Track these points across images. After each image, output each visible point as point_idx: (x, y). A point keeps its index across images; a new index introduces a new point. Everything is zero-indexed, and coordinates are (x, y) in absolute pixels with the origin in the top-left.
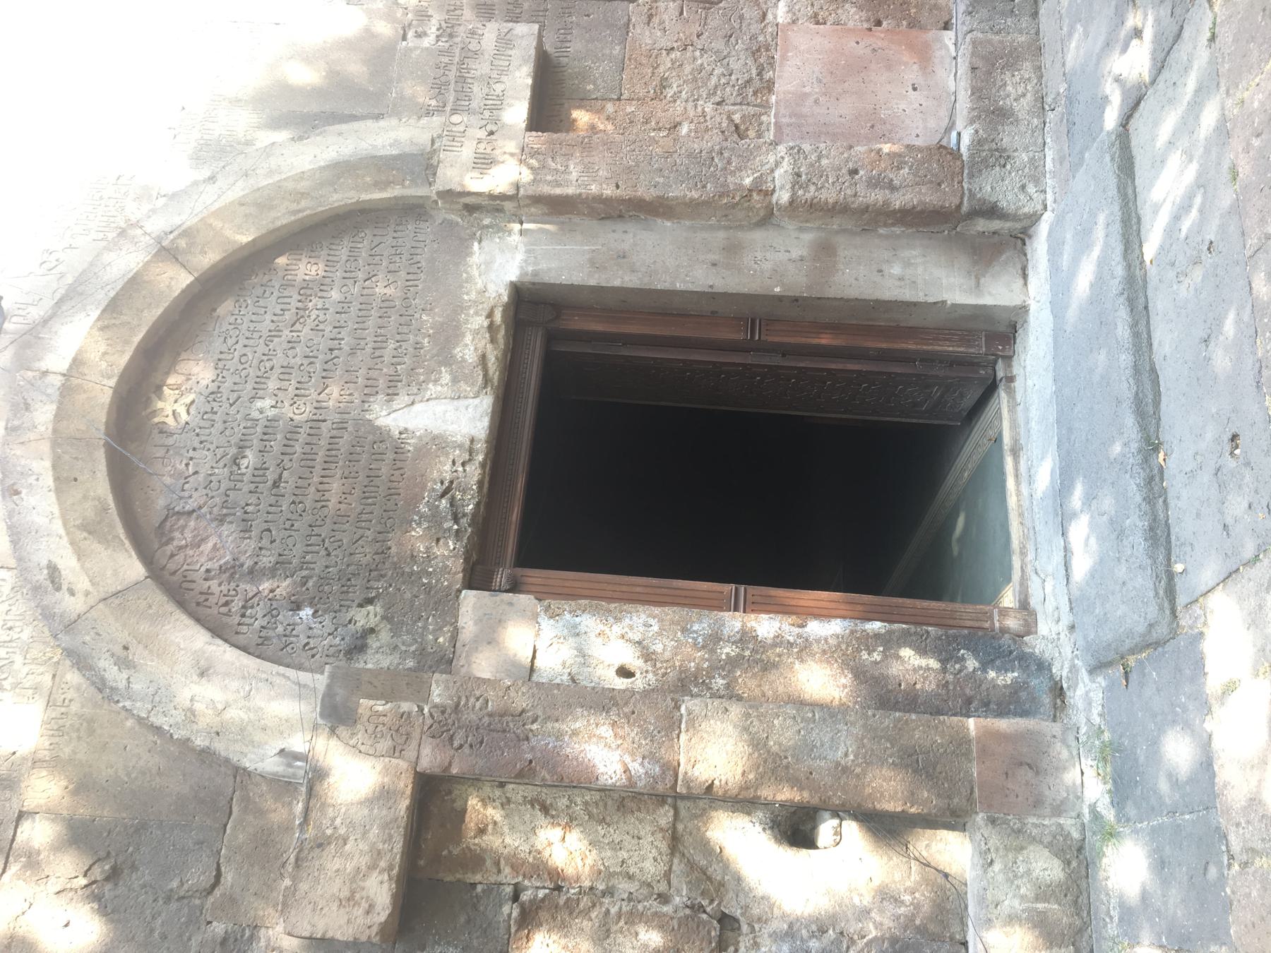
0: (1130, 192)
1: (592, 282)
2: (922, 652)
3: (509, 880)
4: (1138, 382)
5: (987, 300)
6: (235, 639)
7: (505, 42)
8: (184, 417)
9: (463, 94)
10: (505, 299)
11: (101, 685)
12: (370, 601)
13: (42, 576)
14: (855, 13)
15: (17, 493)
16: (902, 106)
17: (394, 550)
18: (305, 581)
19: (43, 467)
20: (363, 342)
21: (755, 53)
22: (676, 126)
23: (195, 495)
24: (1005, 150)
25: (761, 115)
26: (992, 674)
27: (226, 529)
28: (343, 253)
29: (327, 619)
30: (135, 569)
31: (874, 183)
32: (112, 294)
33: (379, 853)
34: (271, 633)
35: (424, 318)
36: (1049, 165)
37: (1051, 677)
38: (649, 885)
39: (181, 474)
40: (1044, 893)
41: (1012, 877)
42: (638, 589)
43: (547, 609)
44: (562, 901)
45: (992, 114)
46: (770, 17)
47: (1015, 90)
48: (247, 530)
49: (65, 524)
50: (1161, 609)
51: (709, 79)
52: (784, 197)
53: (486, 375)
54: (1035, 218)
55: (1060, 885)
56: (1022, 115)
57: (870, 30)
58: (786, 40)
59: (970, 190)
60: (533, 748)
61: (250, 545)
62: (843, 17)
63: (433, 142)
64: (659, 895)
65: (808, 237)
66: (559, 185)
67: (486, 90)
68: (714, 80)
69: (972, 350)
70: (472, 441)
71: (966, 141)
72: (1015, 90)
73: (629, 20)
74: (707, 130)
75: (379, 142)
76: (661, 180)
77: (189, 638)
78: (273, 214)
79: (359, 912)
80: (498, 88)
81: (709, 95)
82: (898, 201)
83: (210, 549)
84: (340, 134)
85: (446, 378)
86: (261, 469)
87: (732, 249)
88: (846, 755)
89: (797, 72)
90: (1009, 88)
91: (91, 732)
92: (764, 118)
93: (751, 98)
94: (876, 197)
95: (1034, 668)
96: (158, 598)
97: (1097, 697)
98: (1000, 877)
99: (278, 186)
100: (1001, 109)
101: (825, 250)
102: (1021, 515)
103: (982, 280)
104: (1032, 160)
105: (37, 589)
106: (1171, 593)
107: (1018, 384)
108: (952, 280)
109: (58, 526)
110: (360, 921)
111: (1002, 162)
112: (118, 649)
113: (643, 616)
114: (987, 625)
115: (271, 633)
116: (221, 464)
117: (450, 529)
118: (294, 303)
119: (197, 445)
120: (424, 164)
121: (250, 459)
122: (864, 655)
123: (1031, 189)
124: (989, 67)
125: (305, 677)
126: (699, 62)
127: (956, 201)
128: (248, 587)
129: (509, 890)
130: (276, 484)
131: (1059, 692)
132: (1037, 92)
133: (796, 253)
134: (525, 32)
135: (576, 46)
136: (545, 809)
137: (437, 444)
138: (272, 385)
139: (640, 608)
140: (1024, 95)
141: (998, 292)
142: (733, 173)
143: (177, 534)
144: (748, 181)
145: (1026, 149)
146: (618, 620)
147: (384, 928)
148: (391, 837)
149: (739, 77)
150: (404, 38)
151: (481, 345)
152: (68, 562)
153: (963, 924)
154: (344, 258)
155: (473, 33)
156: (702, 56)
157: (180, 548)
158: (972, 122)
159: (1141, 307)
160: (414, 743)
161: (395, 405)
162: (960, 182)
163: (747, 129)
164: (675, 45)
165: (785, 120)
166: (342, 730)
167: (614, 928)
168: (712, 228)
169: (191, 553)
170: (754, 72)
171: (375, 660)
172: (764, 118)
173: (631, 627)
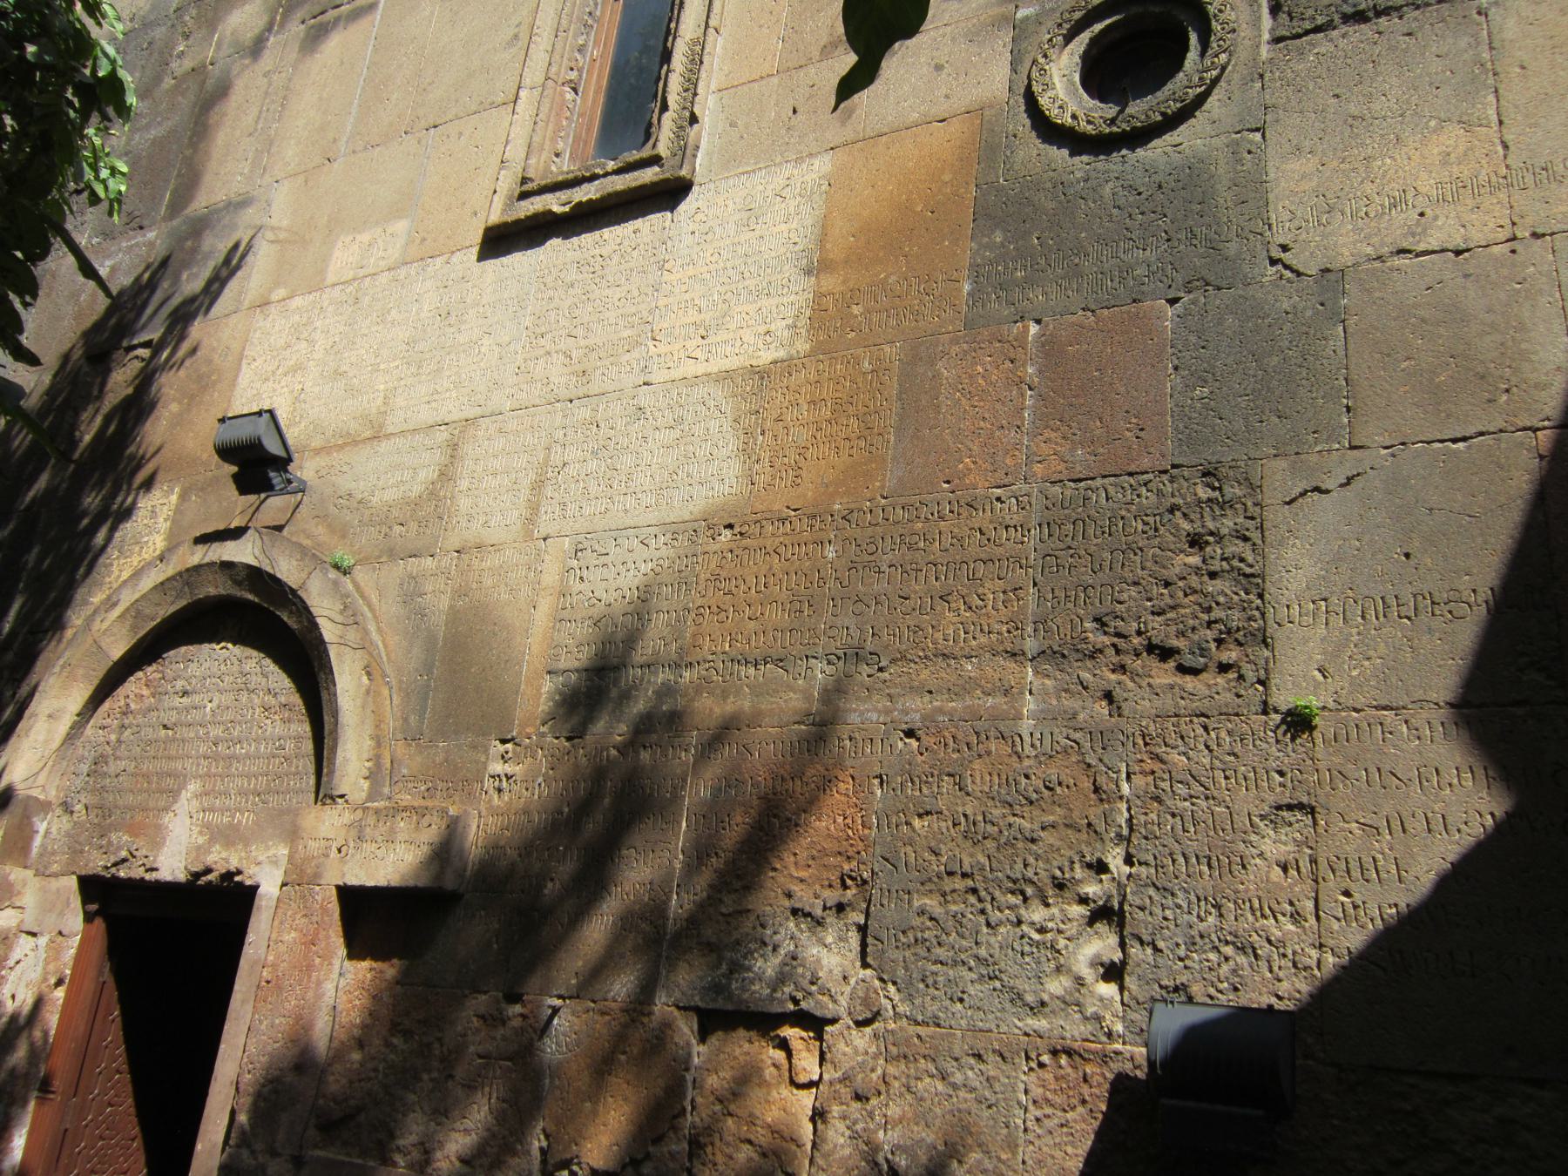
63: (342, 796)
85: (201, 840)
151: (218, 867)
156: (431, 1080)
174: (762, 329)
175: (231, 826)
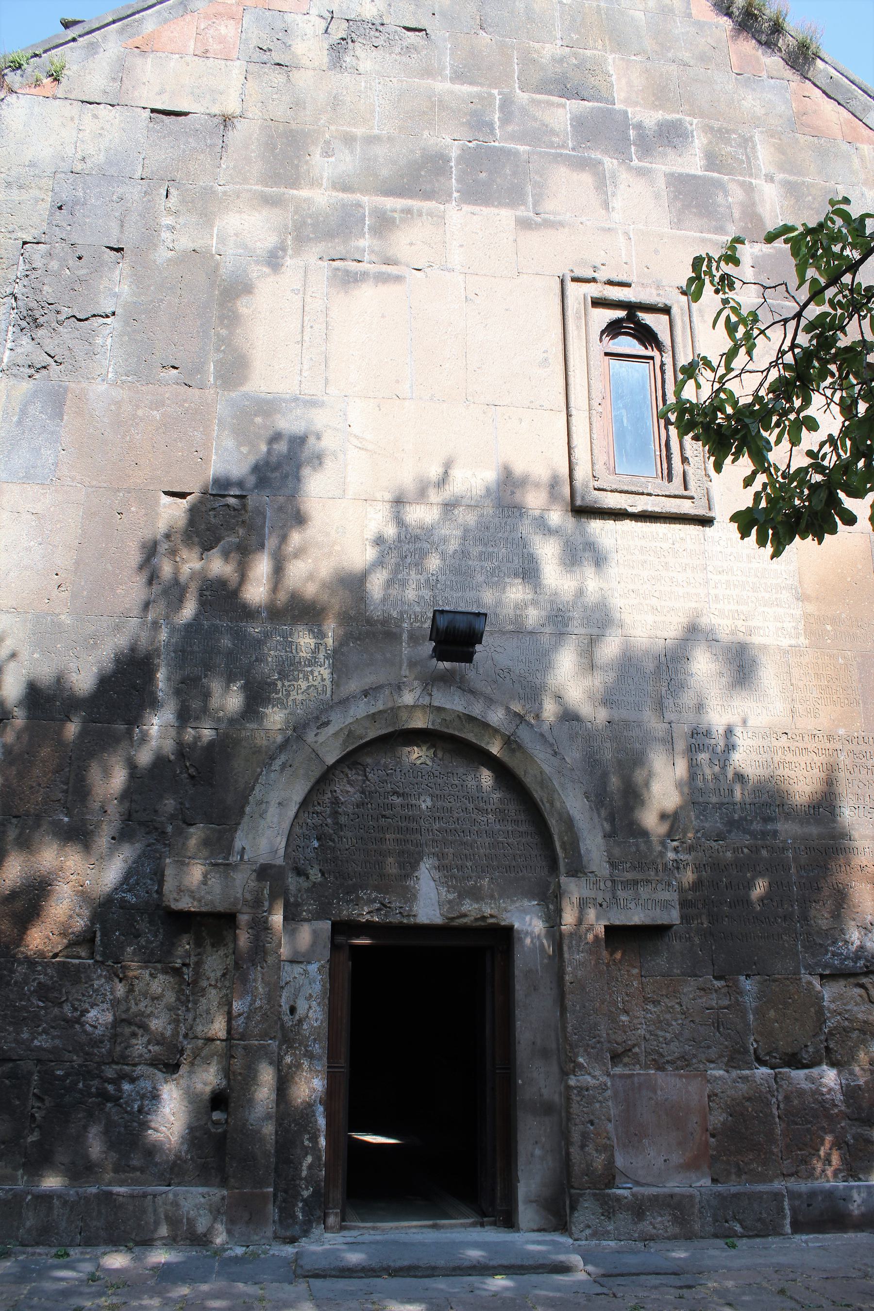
0: (541, 1271)
1: (517, 972)
2: (310, 1167)
3: (192, 961)
4: (427, 1268)
5: (521, 1207)
6: (301, 811)
7: (666, 905)
8: (419, 762)
9: (626, 884)
10: (503, 923)
11: (273, 758)
12: (323, 875)
13: (324, 719)
14: (719, 1121)
15: (366, 697)
16: (652, 1154)
17: (350, 882)
18: (333, 841)
19: (381, 707)
20: (469, 848)
21: (682, 1058)
22: (626, 1012)
23: (375, 777)
24: (614, 1215)
25: (640, 1065)
26: (300, 1205)
27: (358, 796)
28: (523, 828)
29: (313, 855)
30: (331, 760)
31: (585, 1136)
32: (479, 717)
33: (200, 901)
34: (304, 828)
35: (487, 880)
36: (604, 1243)
37: (300, 1237)
38: (191, 1029)
39: (387, 767)
40: (191, 1222)
41: (198, 1207)
42: (339, 1014)
43: (323, 966)
44: (183, 987)
45: (639, 1209)
46: (712, 1066)
47: (659, 1222)
48: (358, 807)
49: (351, 723)
50: (309, 1271)
51: (662, 1030)
52: (572, 1082)
53: (454, 918)
54: (571, 1235)
55: (195, 1231)
56: (640, 1226)
57: (707, 1130)
58: (695, 1076)
59: (584, 1194)
60: (248, 968)
61: (350, 809)
62: (716, 1113)
63: (593, 872)
64: (187, 1034)
65: (556, 1098)
66: (569, 948)
67: (629, 898)
68: (660, 1033)
69: (499, 1201)
70: (414, 916)
71: (619, 1192)
72: (659, 1222)
73: (700, 977)
74: (625, 1032)
75: (588, 842)
76: (578, 1008)
77: (298, 792)
78: (539, 789)
79: (175, 895)
80: (632, 905)
81: (650, 1032)
82: (574, 1150)
83: (346, 790)
84: (591, 819)
85: (451, 897)
86: (392, 806)
87: (545, 1053)
88: (252, 1125)
89: (670, 1085)
90: (659, 1219)
91: (254, 753)
92: (638, 1066)
93: (650, 1058)
94: (576, 1137)
95: (305, 1228)
96: (317, 773)
97: (283, 1254)
98: (197, 1201)
99: (554, 790)
100: (643, 1213)
101: (548, 1109)
102: (397, 1228)
103: (534, 1204)
104: (608, 1232)
105: (317, 718)
106: (316, 1276)
107: (479, 1229)
108: (534, 1186)
109: (350, 720)
110: (171, 896)
111: (606, 1214)
112: (290, 762)
113: (321, 1017)
114: (331, 1205)
115: (304, 828)
116: (393, 786)
117: (363, 910)
118: (489, 807)
119: (403, 772)
120: (577, 870)
121: (397, 800)
122: (307, 1136)
123: (588, 1232)
124: (677, 1207)
125: (282, 852)
126: (674, 1023)
127: (576, 1185)
128: (328, 812)
129: (187, 961)
130: (384, 816)
131: (292, 1240)
132: (657, 1236)
133: (545, 1091)
134: (674, 916)
135: (677, 945)
136: (224, 975)
137: (409, 896)
138: (439, 804)
139: (326, 1016)
140: (655, 1228)
141: (526, 1214)
142: (586, 1050)
143: (354, 772)
144: (581, 1060)
145: (616, 1229)
146: (319, 1004)
147: (168, 907)
148: (207, 905)
149: (664, 1049)
150: (672, 841)
152: (331, 730)
153: (179, 1184)
154: (521, 830)
155: (669, 884)
156: (678, 1024)
157: (347, 775)
158: (633, 1195)
159: (470, 1272)
160: (249, 910)
161: (433, 872)
162: (589, 1188)
163: (629, 1057)
164: (684, 1007)
165: (636, 1079)
166: (254, 875)
167: (172, 1013)
168: (558, 1040)
169: (345, 780)
170: (669, 1058)
171: (292, 882)
172: (638, 1066)
173: (315, 1011)
174: (779, 625)
175: (475, 886)
